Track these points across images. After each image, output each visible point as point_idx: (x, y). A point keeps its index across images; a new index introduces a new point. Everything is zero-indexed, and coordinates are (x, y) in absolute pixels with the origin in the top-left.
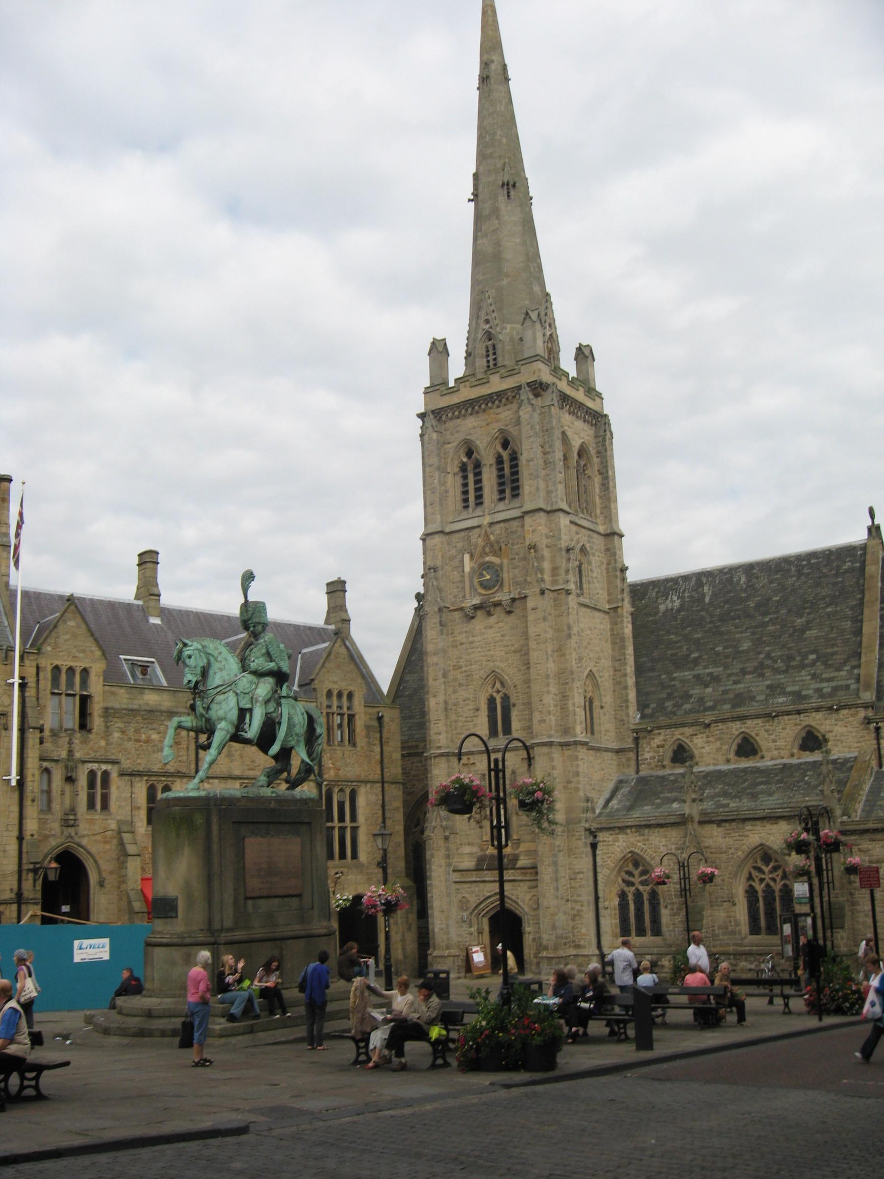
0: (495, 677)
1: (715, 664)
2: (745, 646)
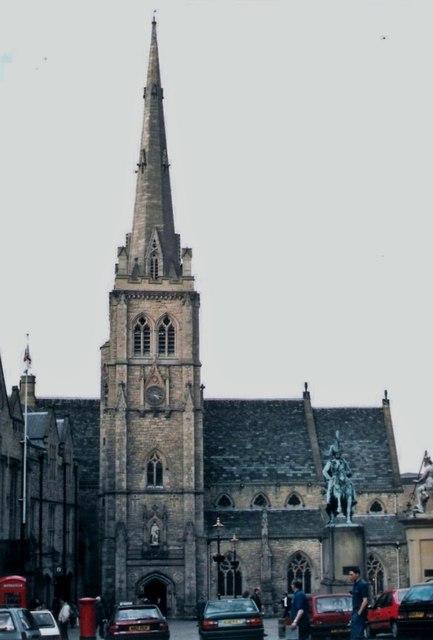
1: (234, 454)
2: (249, 446)
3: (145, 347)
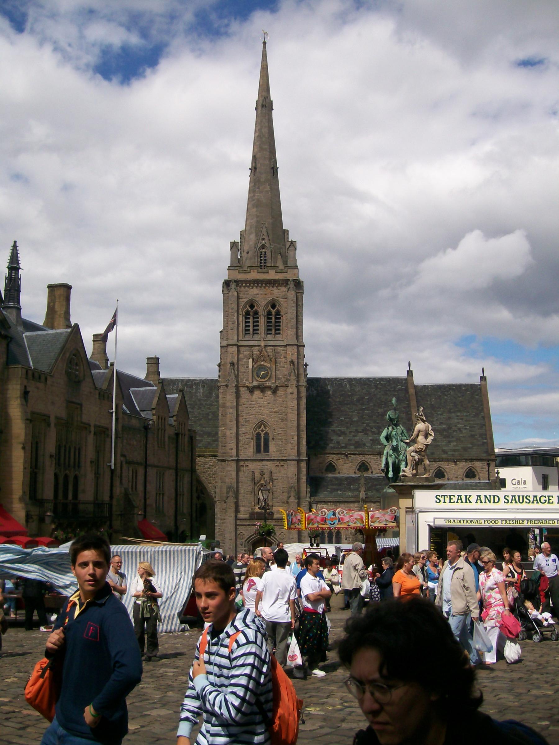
0: (262, 423)
3: (254, 330)
